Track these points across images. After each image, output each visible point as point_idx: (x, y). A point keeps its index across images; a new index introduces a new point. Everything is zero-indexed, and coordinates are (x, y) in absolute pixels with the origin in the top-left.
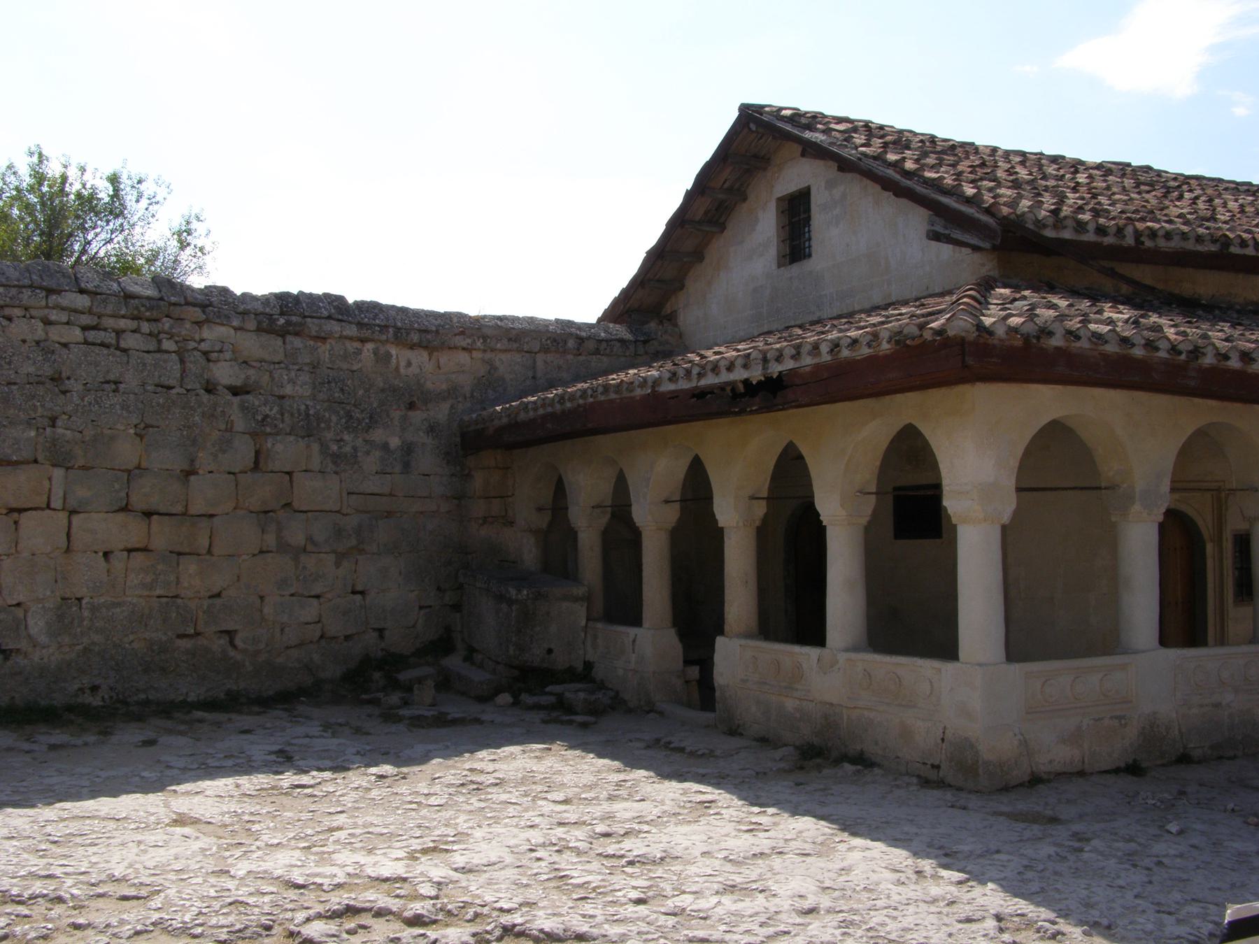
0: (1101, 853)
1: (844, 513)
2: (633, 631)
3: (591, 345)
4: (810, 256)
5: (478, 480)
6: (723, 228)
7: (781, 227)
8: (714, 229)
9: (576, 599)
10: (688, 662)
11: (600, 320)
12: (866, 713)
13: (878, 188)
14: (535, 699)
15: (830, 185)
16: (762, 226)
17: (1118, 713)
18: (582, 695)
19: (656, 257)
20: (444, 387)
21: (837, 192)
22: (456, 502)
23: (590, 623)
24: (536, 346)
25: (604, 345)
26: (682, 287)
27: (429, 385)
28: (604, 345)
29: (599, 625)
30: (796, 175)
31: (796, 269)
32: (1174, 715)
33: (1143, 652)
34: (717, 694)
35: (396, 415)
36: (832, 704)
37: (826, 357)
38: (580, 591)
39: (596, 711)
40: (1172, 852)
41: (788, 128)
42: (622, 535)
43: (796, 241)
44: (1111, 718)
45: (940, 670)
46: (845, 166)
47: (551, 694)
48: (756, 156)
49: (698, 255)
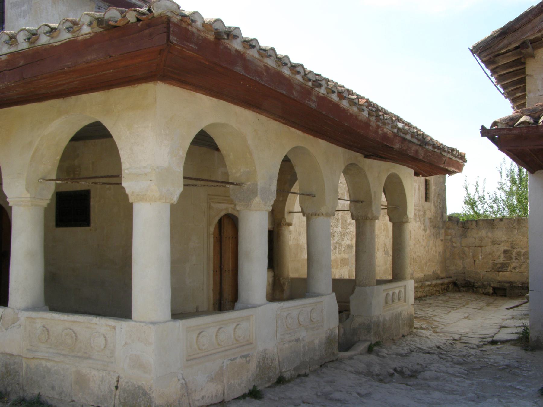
1: (28, 195)
12: (44, 363)
17: (245, 353)
32: (276, 350)
33: (260, 306)
36: (12, 355)
37: (23, 45)
44: (241, 357)
45: (114, 328)
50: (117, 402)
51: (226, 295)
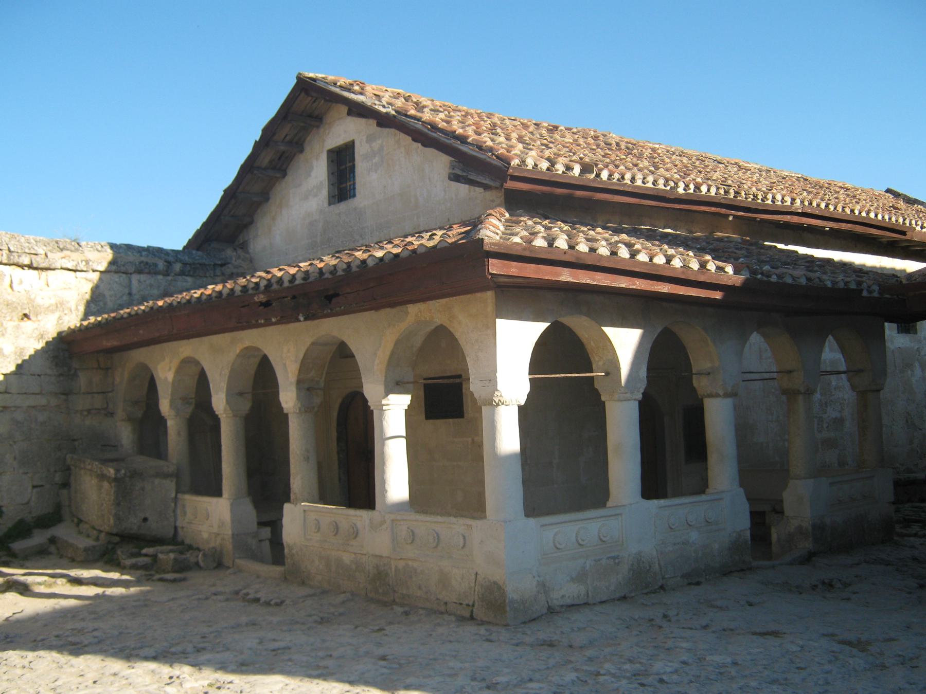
0: (614, 675)
2: (214, 500)
3: (178, 267)
4: (354, 196)
5: (83, 379)
6: (284, 174)
7: (331, 173)
8: (278, 175)
9: (166, 476)
10: (261, 524)
11: (185, 248)
13: (407, 140)
14: (133, 560)
15: (370, 139)
16: (316, 172)
17: (613, 554)
18: (172, 556)
19: (230, 195)
20: (53, 301)
21: (376, 145)
22: (63, 397)
23: (179, 496)
24: (132, 270)
25: (188, 268)
26: (251, 223)
27: (39, 301)
28: (188, 268)
29: (188, 497)
30: (342, 130)
31: (343, 206)
32: (655, 553)
34: (286, 551)
35: (10, 325)
36: (381, 557)
38: (172, 469)
39: (182, 567)
40: (668, 670)
41: (337, 90)
42: (202, 422)
43: (342, 182)
44: (608, 558)
46: (384, 121)
47: (146, 555)
48: (310, 116)
49: (265, 196)
50: (476, 598)
51: (592, 493)
